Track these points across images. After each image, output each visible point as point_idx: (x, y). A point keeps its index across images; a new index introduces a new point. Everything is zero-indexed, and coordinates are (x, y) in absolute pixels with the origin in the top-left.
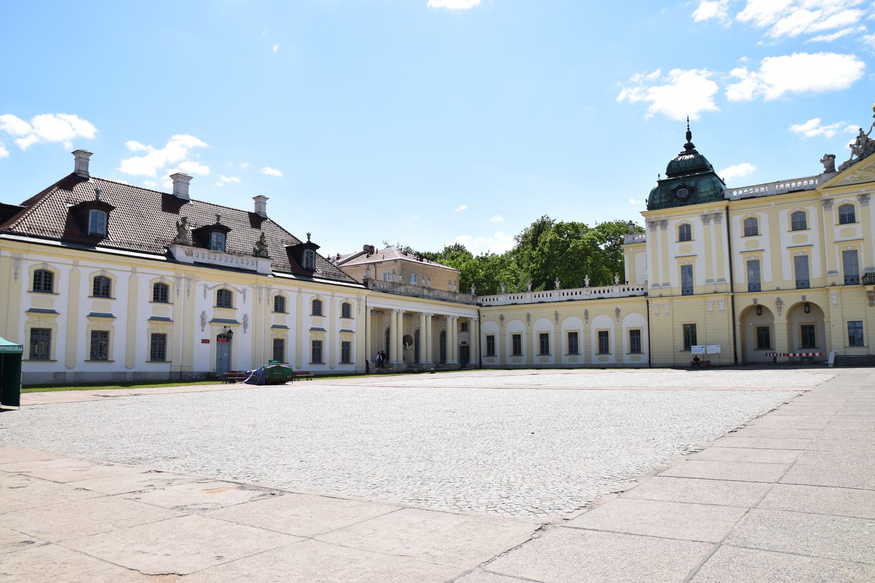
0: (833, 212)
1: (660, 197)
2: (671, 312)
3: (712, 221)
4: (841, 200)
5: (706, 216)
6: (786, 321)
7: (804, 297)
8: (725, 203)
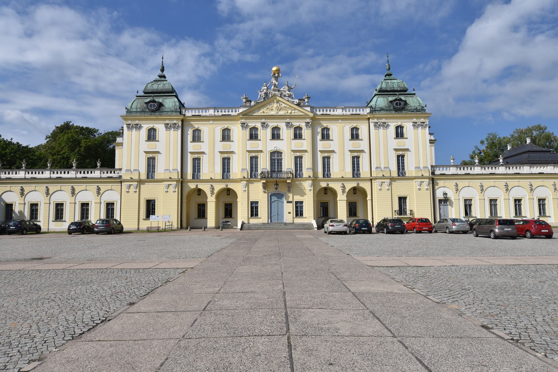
0: (247, 131)
1: (137, 107)
2: (138, 190)
6: (214, 200)
8: (182, 117)
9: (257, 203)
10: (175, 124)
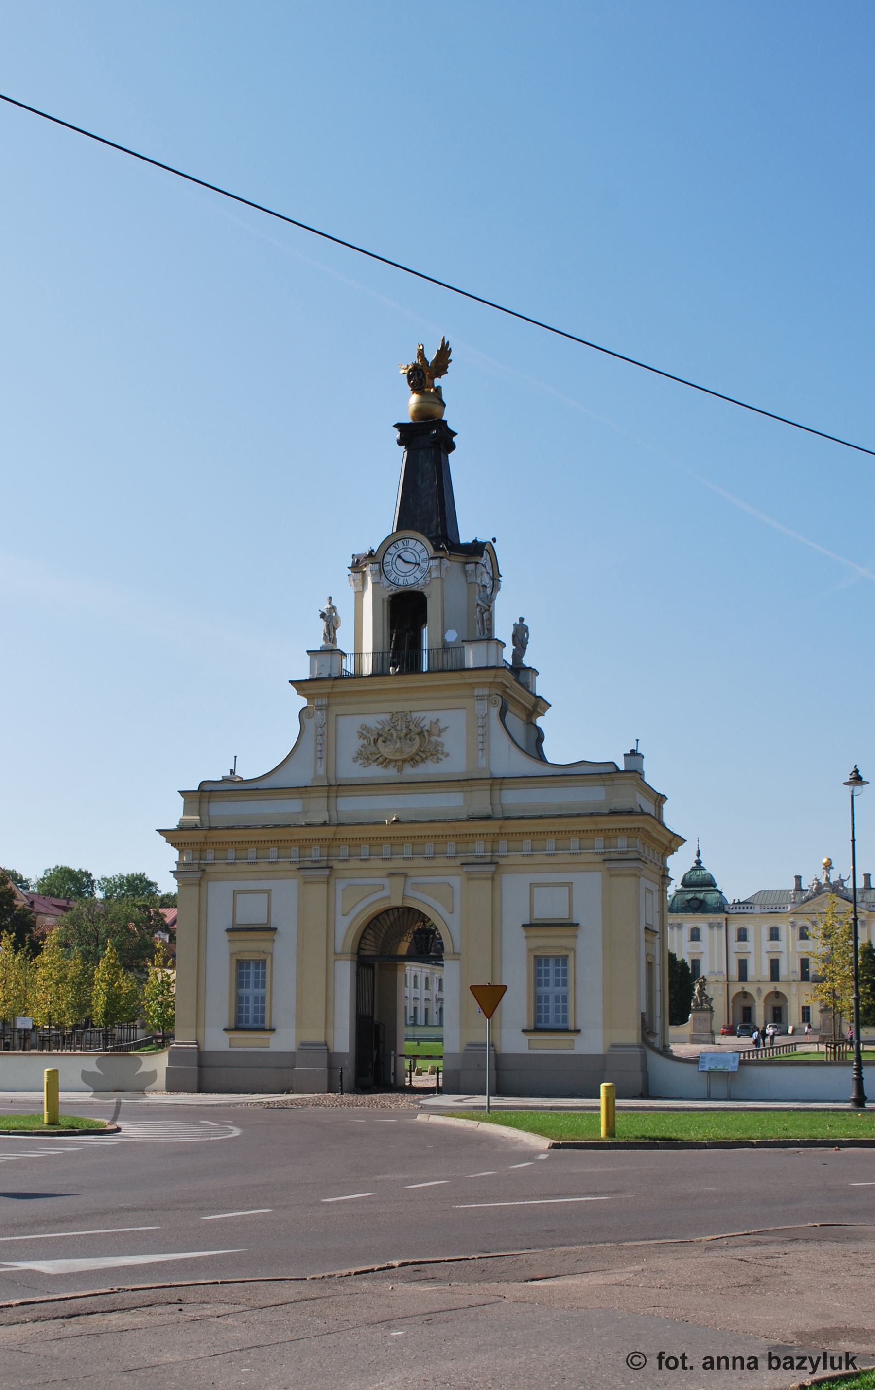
3: (715, 928)
4: (801, 923)
5: (712, 923)
7: (775, 988)
8: (726, 915)
9: (808, 1008)
10: (719, 923)
